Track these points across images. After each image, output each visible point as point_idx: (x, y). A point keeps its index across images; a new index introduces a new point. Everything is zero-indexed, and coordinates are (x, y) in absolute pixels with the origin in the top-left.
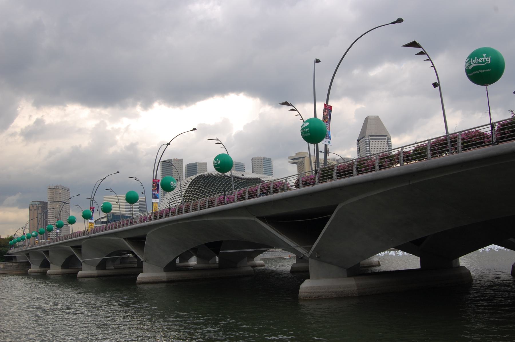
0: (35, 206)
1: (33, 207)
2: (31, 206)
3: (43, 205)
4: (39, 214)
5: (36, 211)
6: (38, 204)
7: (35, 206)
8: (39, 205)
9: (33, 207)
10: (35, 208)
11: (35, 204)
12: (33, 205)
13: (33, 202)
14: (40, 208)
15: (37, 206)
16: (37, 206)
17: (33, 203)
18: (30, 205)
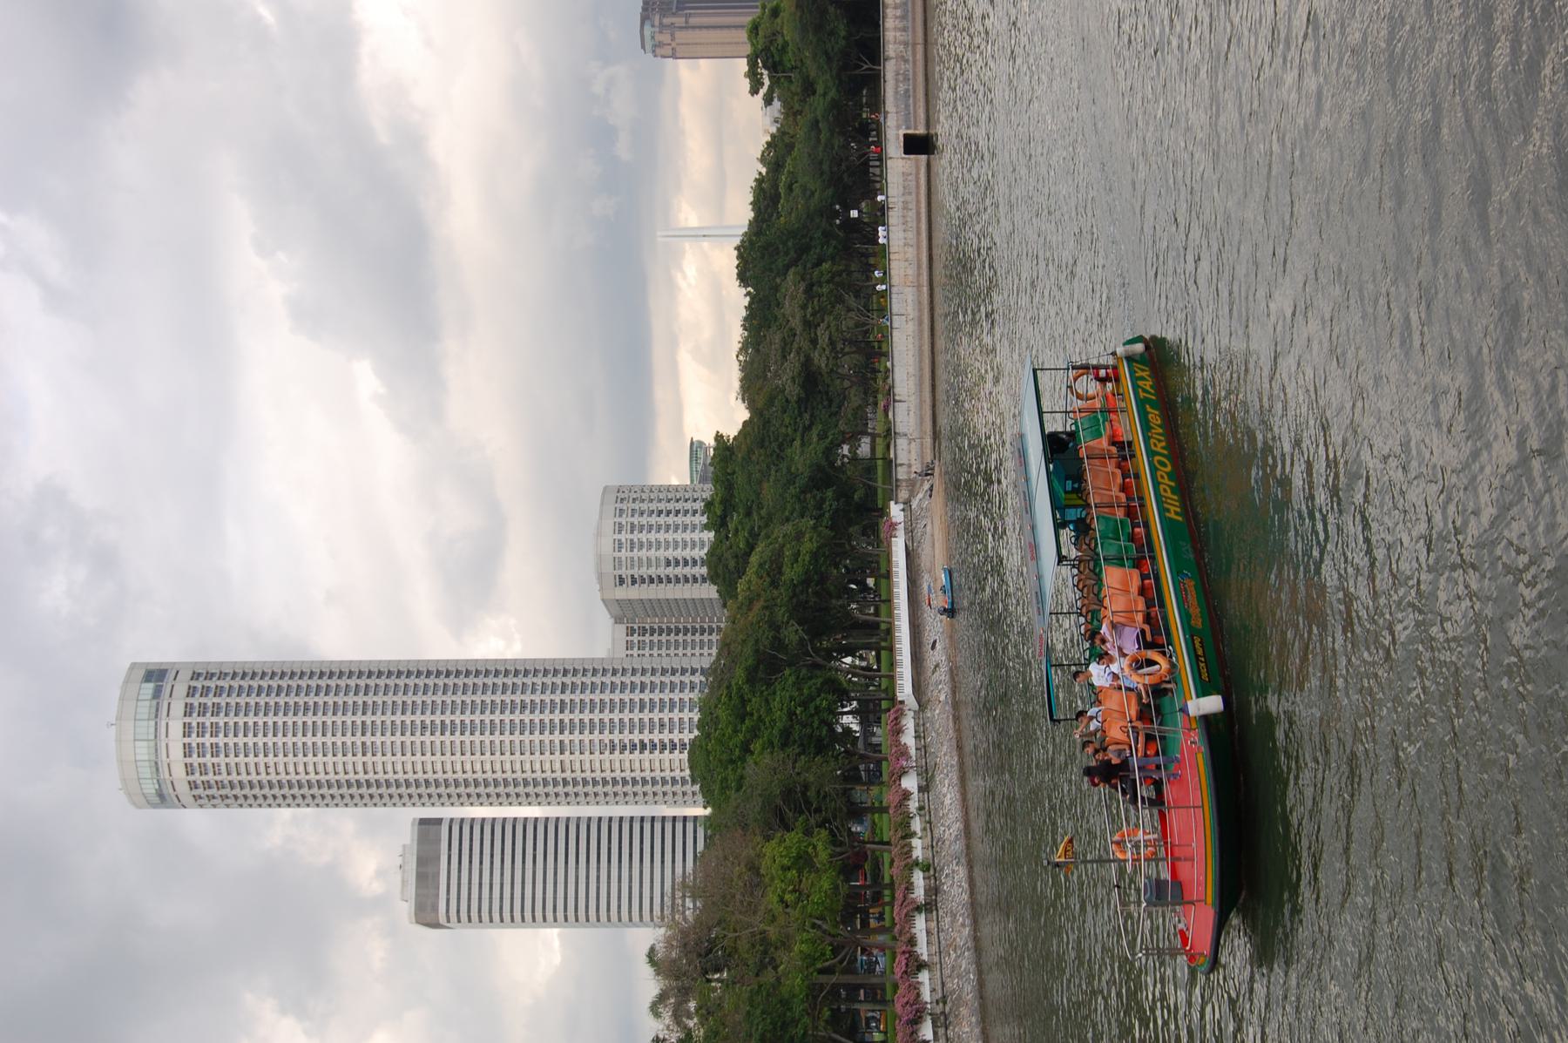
0: (659, 37)
1: (660, 45)
2: (658, 51)
3: (653, 10)
4: (687, 22)
5: (678, 34)
6: (653, 26)
7: (659, 37)
8: (657, 23)
9: (660, 45)
10: (666, 38)
11: (653, 38)
12: (655, 46)
13: (643, 47)
14: (667, 21)
15: (657, 29)
16: (661, 32)
17: (648, 46)
18: (655, 56)
